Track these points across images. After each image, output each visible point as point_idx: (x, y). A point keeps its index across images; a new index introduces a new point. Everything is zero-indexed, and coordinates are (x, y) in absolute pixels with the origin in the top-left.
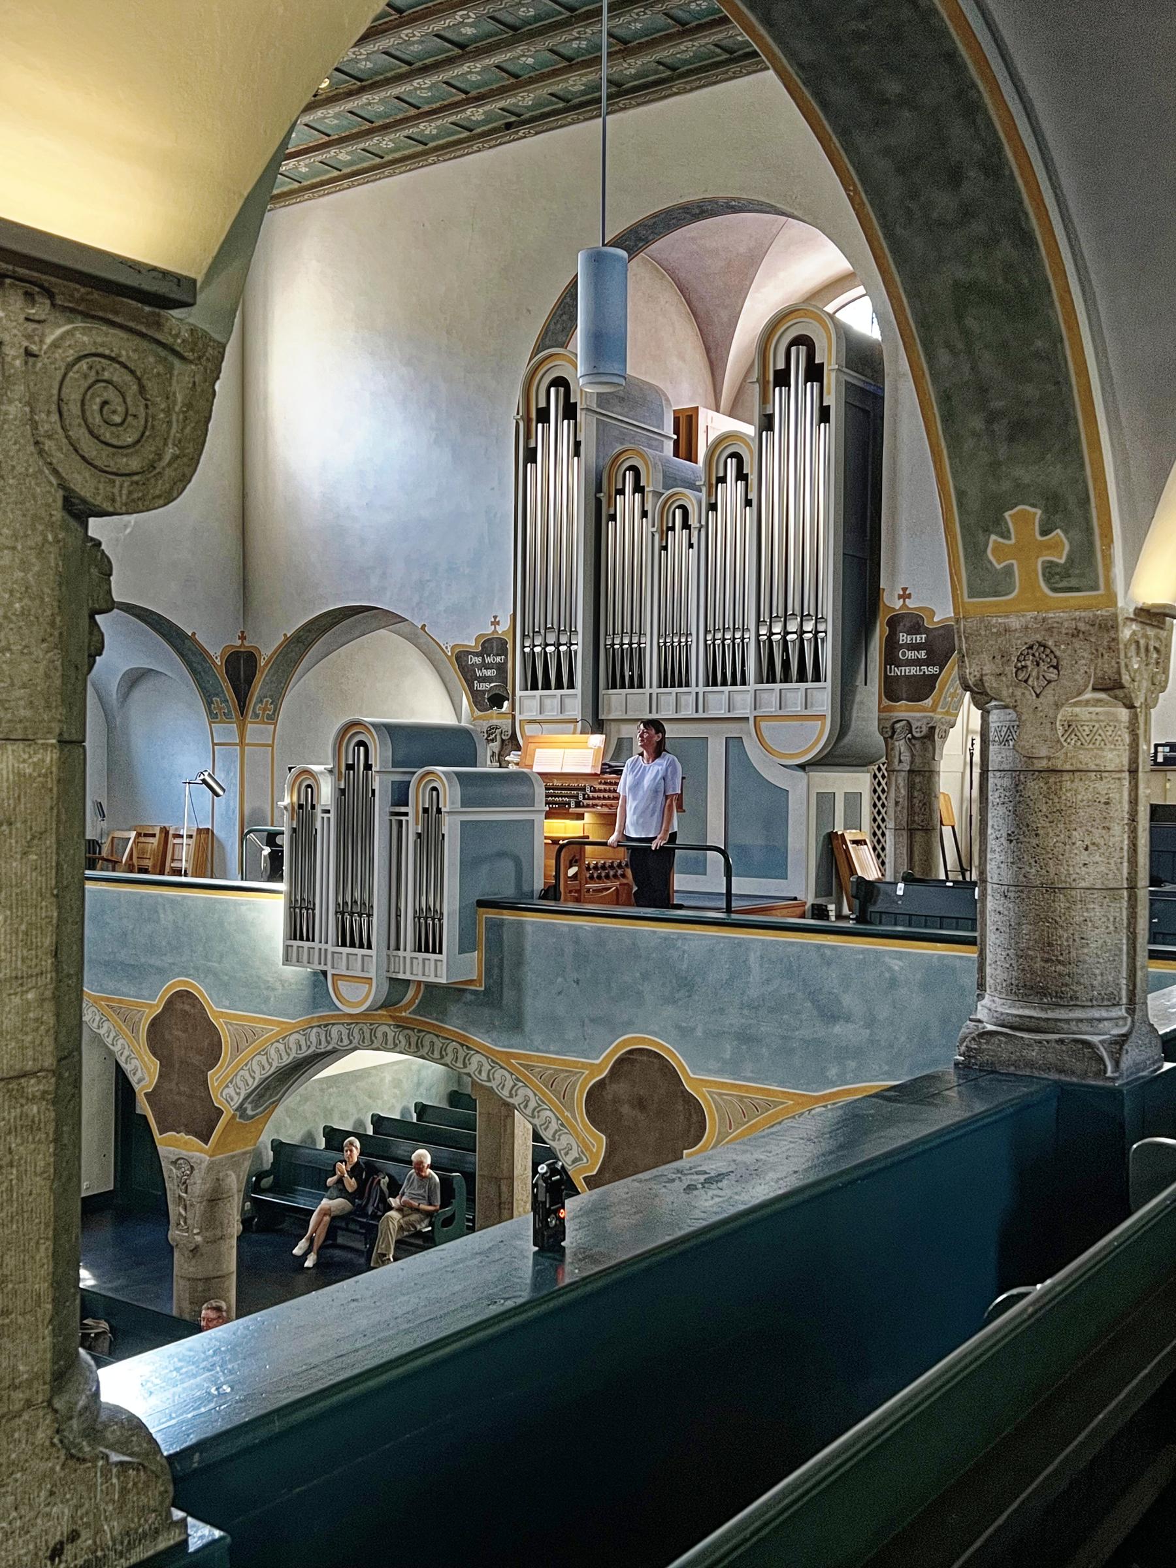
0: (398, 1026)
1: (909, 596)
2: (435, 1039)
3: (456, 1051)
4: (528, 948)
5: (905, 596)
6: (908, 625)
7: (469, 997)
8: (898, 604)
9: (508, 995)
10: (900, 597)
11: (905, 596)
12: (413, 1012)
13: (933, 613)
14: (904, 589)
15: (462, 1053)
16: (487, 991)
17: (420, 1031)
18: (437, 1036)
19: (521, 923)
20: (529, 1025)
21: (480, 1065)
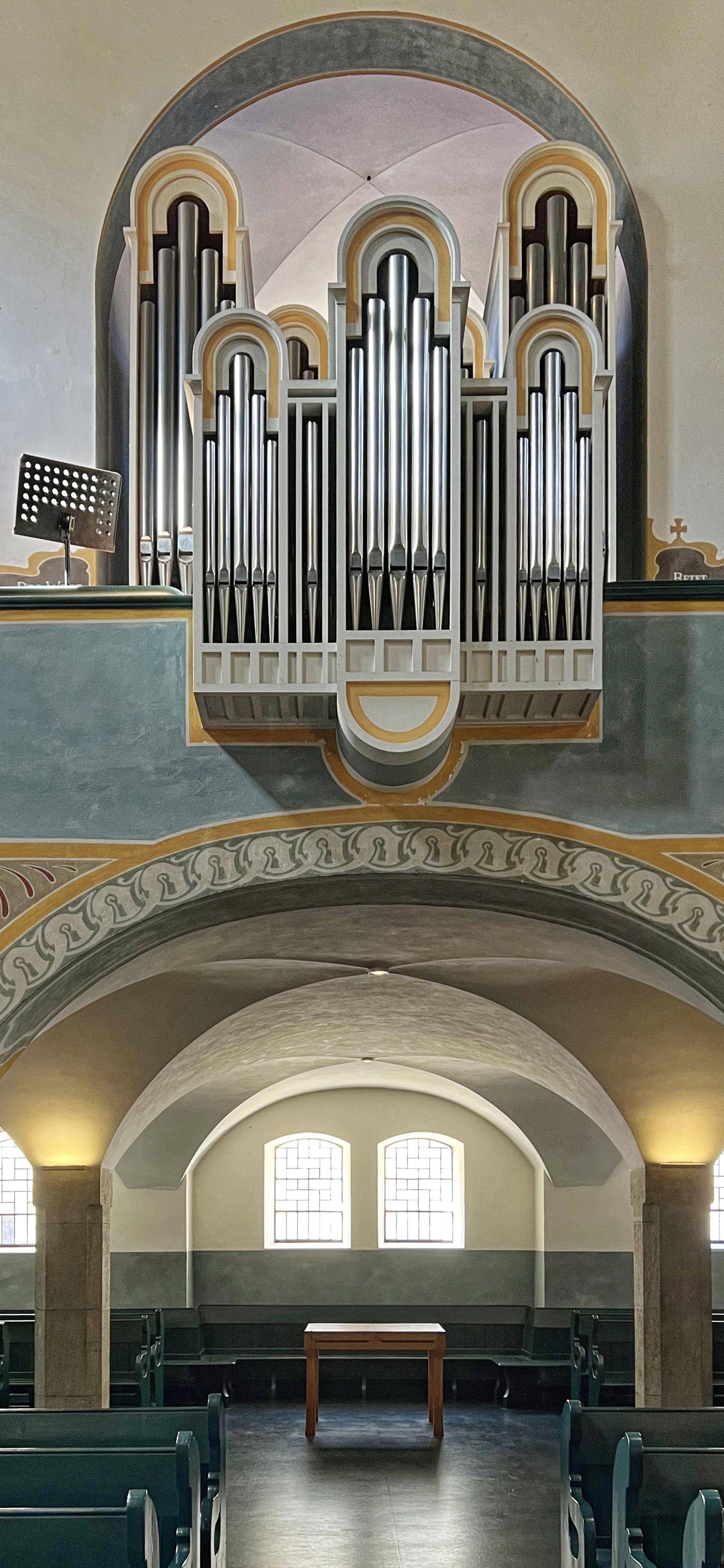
0: (408, 825)
1: (684, 529)
2: (494, 838)
3: (540, 853)
4: (697, 661)
5: (678, 529)
6: (684, 562)
7: (565, 758)
8: (671, 538)
9: (654, 746)
10: (673, 530)
11: (678, 529)
12: (444, 797)
13: (714, 550)
14: (678, 521)
15: (554, 854)
16: (610, 741)
17: (459, 828)
18: (500, 832)
19: (682, 622)
20: (699, 792)
21: (596, 869)
